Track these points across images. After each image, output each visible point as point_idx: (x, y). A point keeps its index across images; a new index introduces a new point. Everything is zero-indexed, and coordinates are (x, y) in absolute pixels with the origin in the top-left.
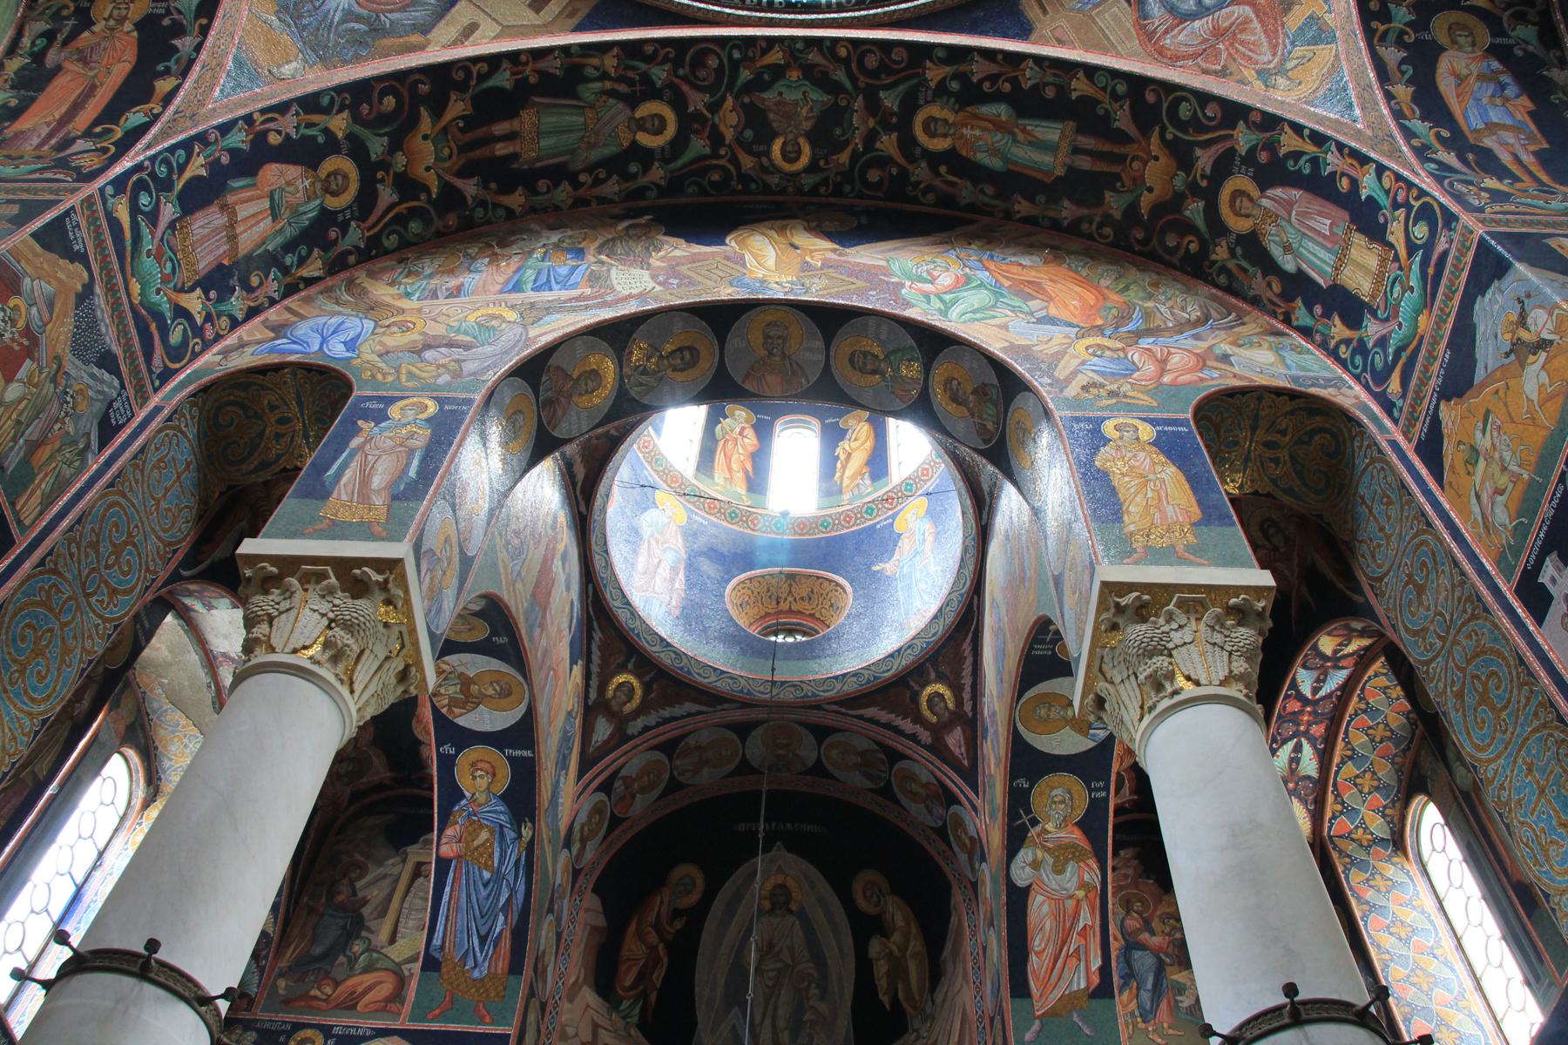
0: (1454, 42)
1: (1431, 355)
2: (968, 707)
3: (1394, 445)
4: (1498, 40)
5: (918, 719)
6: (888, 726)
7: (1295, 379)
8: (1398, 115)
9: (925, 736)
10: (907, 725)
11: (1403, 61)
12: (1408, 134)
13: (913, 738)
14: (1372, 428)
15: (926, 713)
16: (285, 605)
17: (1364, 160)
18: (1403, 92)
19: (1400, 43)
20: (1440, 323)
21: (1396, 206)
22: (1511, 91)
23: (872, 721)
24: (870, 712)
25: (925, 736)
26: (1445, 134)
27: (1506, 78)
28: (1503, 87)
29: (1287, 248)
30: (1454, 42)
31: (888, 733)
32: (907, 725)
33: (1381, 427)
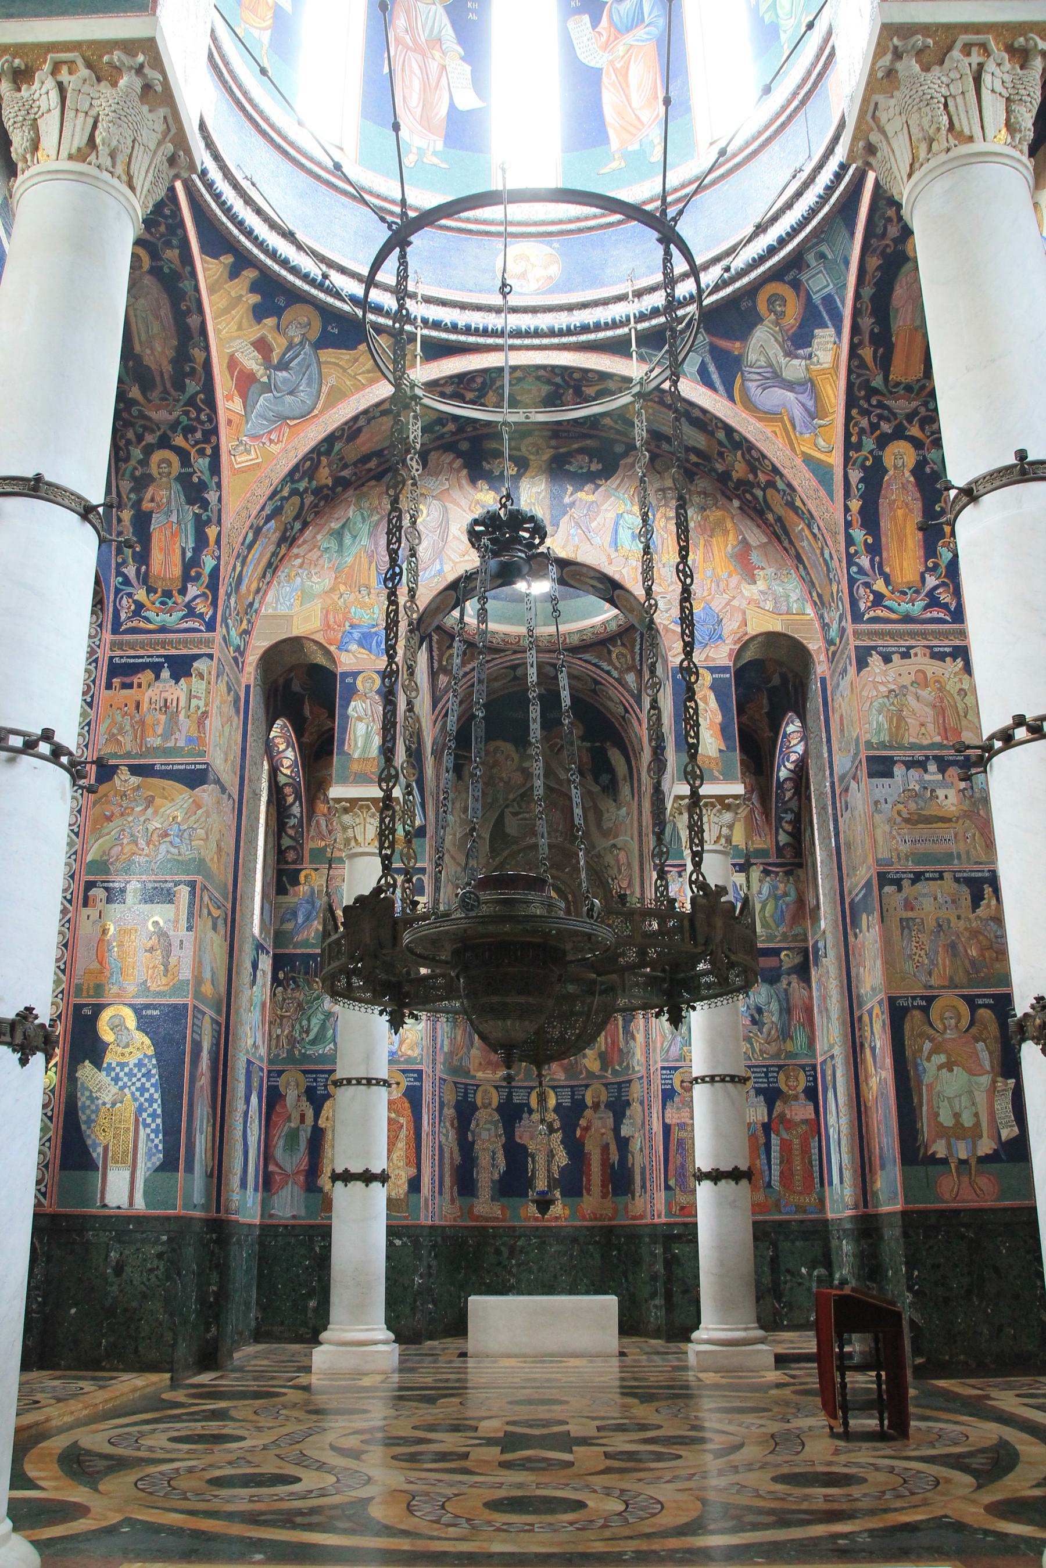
2: (638, 663)
5: (610, 662)
6: (595, 665)
8: (848, 525)
9: (615, 674)
10: (605, 665)
11: (861, 480)
12: (850, 541)
13: (608, 673)
15: (615, 661)
16: (358, 821)
18: (855, 505)
19: (863, 467)
23: (586, 661)
24: (587, 656)
25: (615, 674)
26: (870, 540)
31: (594, 669)
32: (605, 665)
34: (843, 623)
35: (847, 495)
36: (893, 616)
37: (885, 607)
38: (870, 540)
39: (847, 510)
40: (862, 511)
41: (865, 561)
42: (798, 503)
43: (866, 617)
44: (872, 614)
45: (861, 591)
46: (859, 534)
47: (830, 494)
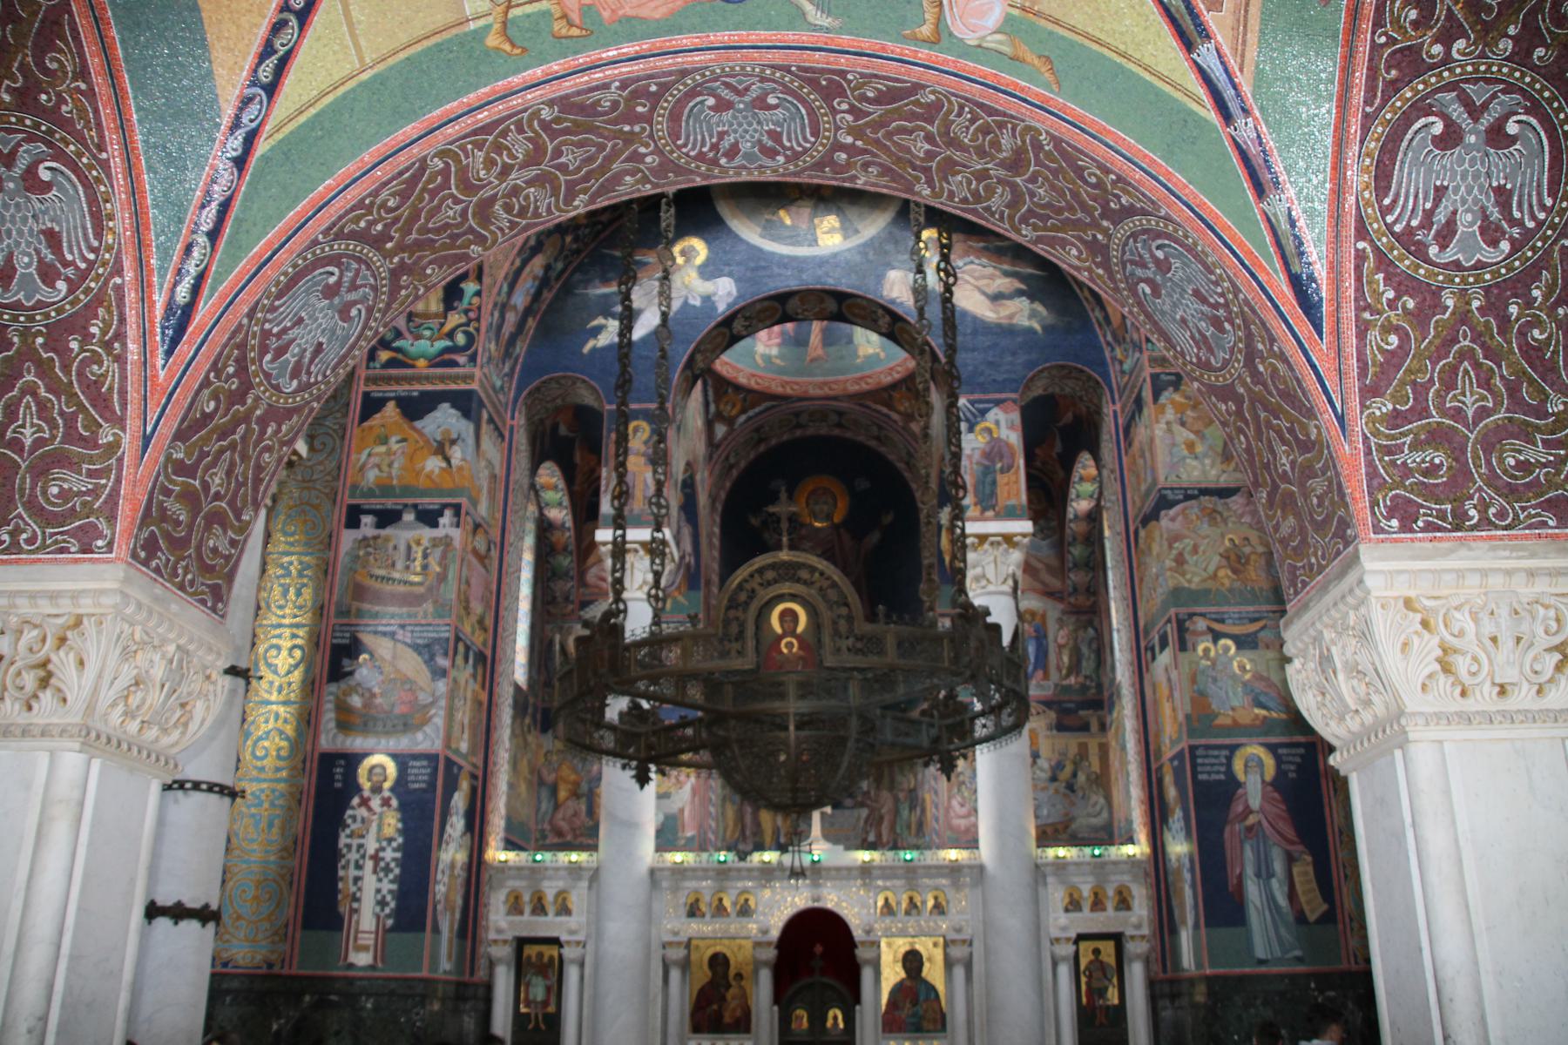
17: (479, 278)
21: (466, 312)
34: (462, 359)
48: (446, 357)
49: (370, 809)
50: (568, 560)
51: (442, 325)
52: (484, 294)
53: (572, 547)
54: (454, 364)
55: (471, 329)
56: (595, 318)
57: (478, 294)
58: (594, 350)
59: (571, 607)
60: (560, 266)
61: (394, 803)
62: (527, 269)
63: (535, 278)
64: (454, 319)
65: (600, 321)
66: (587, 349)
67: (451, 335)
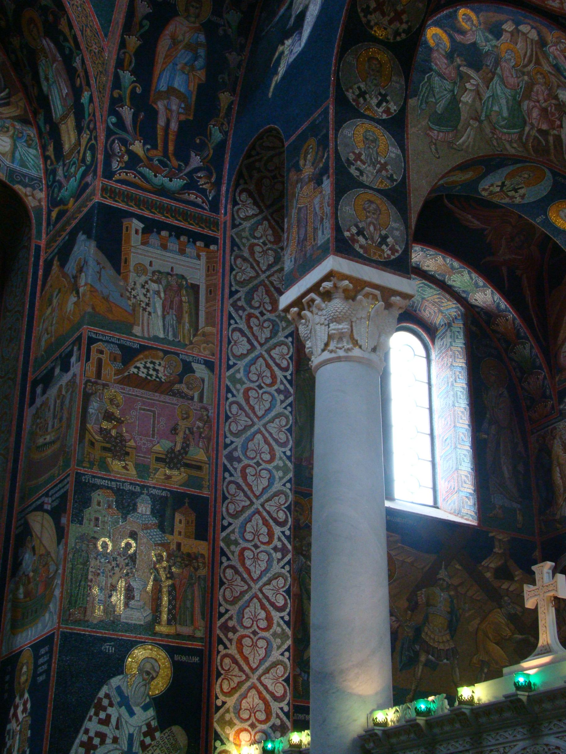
0: (187, 10)
1: (68, 223)
3: (38, 248)
4: (214, 18)
7: (11, 173)
8: (120, 64)
11: (147, 17)
12: (117, 83)
14: (34, 231)
17: (88, 84)
18: (133, 42)
20: (79, 210)
21: (88, 128)
22: (200, 63)
26: (139, 91)
27: (202, 52)
28: (196, 58)
29: (47, 79)
30: (187, 10)
33: (39, 233)
34: (89, 179)
35: (127, 28)
36: (149, 187)
37: (140, 173)
38: (139, 91)
39: (123, 44)
40: (138, 53)
41: (127, 112)
42: (63, 26)
43: (117, 177)
44: (123, 176)
45: (116, 145)
46: (127, 77)
47: (106, 22)
48: (83, 182)
49: (17, 719)
50: (528, 346)
51: (79, 152)
52: (96, 100)
53: (524, 330)
54: (87, 185)
55: (93, 142)
56: (276, 49)
57: (91, 100)
58: (276, 85)
59: (550, 403)
60: (233, 17)
61: (29, 706)
62: (164, 44)
63: (191, 47)
64: (85, 136)
65: (281, 48)
66: (270, 95)
67: (84, 160)
